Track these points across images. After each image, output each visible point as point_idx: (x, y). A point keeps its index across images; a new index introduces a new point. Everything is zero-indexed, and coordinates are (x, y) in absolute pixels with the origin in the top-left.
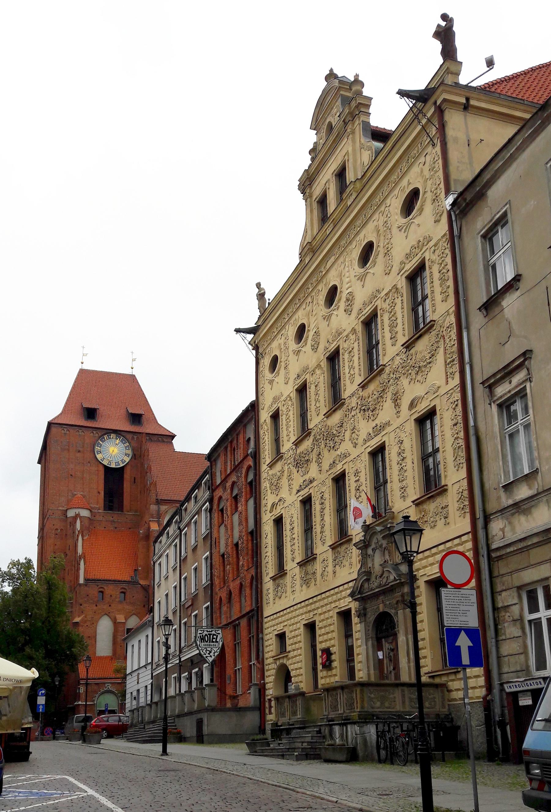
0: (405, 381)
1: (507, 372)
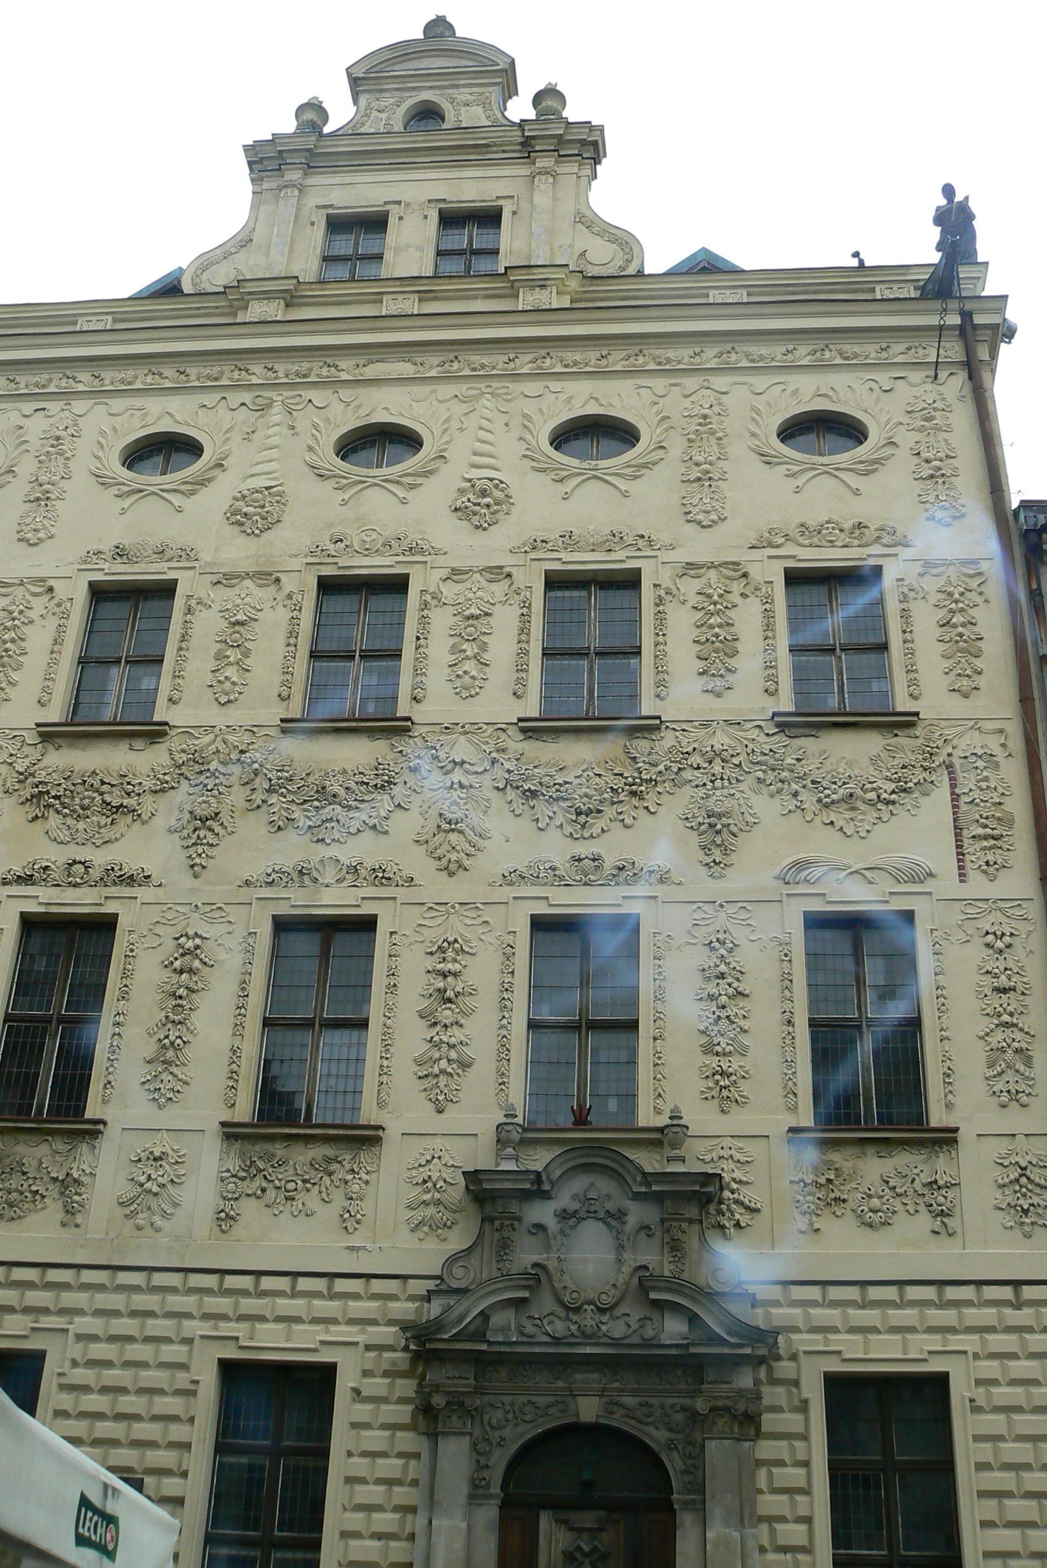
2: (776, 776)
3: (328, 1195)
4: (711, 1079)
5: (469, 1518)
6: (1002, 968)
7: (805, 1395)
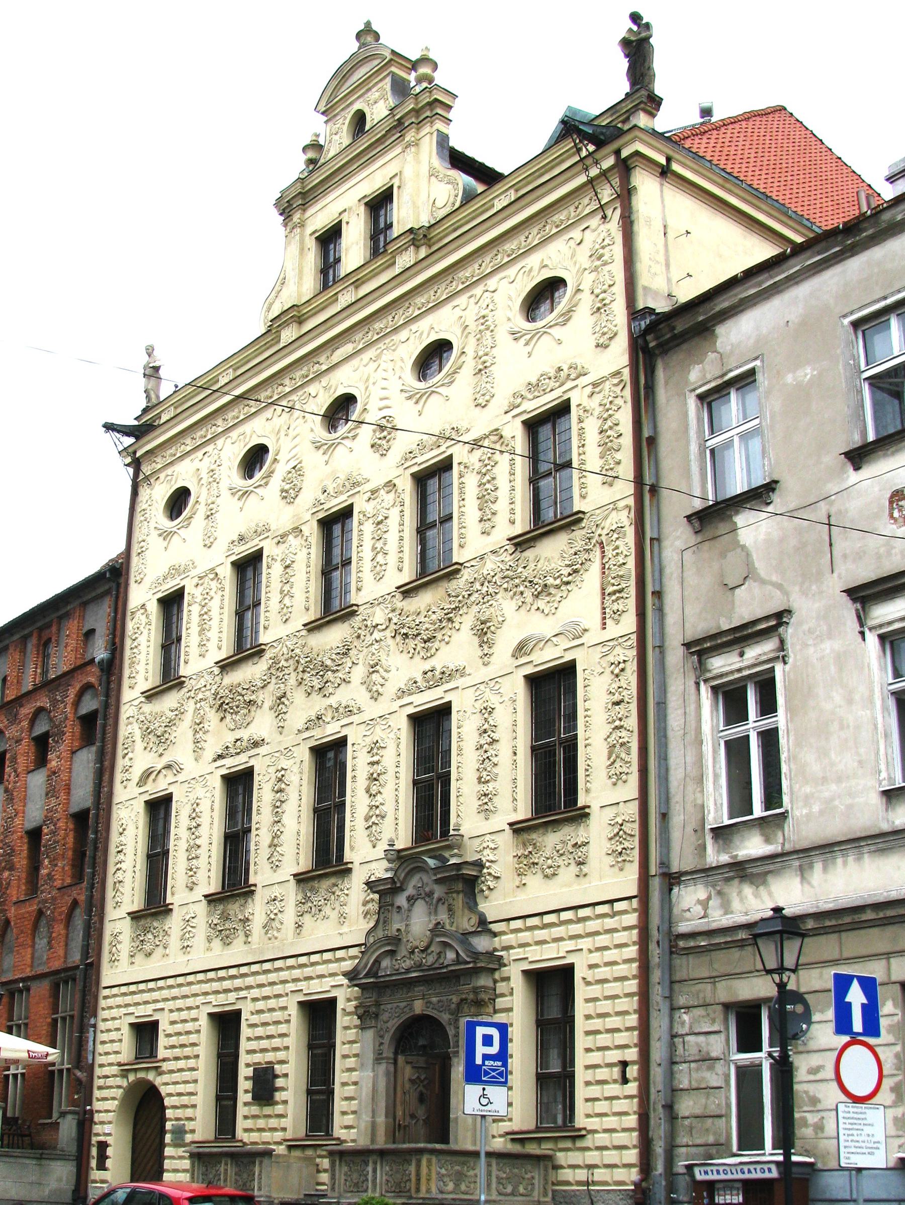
0: (506, 605)
1: (741, 636)
2: (512, 582)
5: (373, 1071)
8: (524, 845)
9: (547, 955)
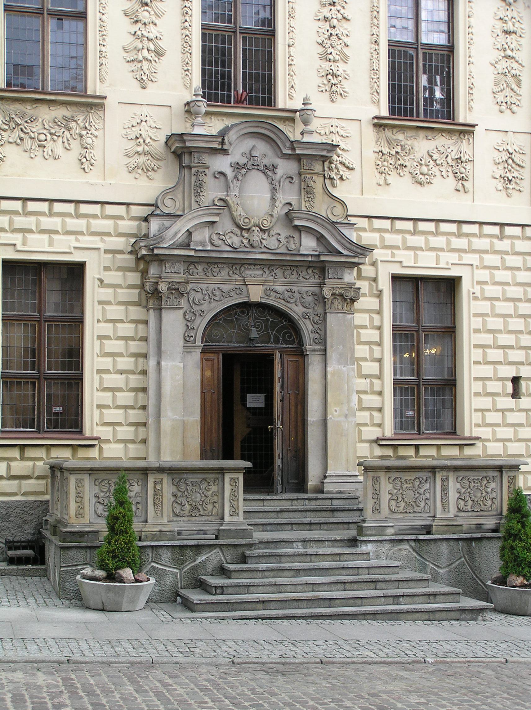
3: (69, 144)
4: (325, 78)
5: (183, 360)
6: (510, 17)
7: (380, 287)
8: (389, 142)
9: (427, 264)
